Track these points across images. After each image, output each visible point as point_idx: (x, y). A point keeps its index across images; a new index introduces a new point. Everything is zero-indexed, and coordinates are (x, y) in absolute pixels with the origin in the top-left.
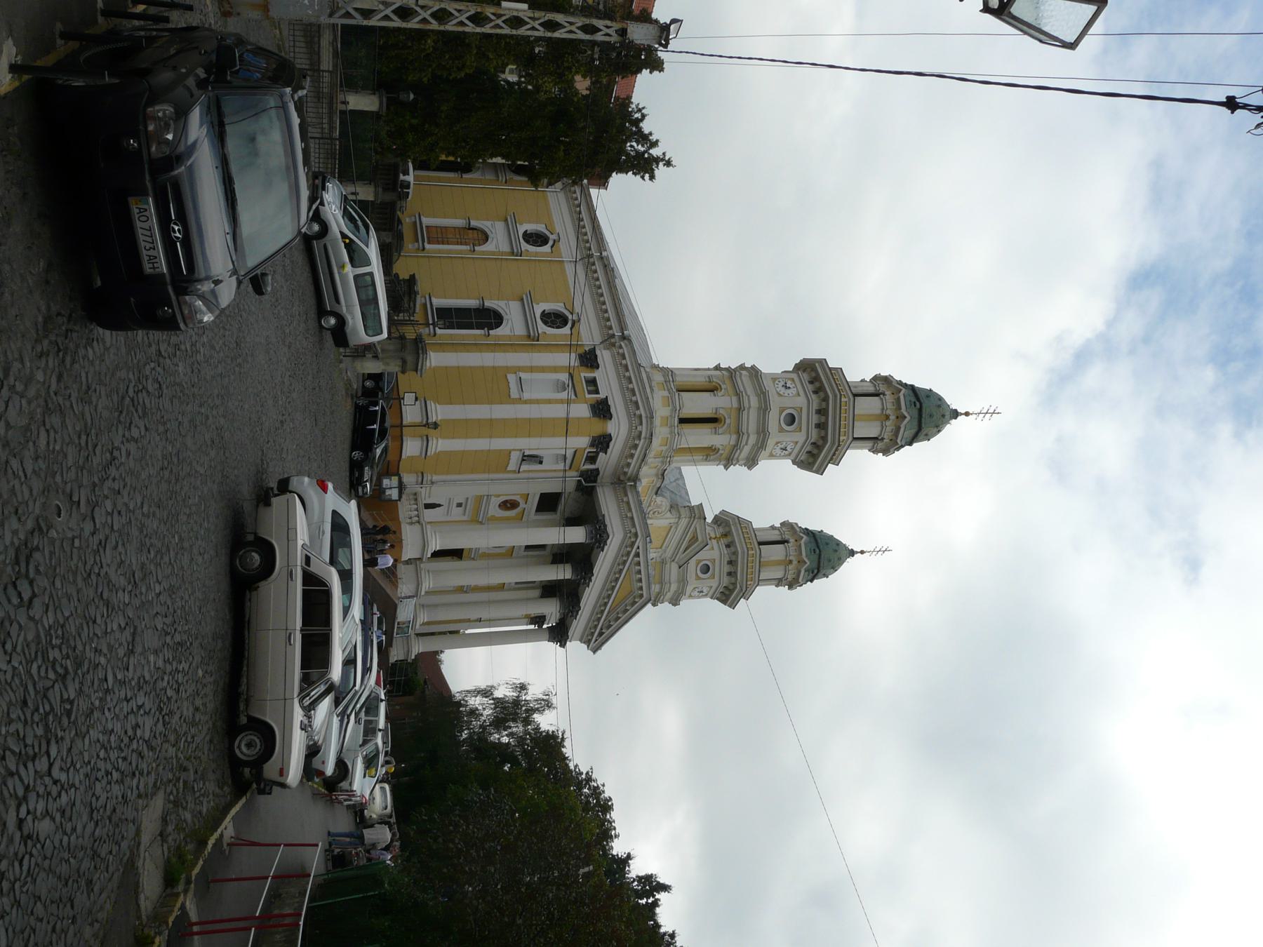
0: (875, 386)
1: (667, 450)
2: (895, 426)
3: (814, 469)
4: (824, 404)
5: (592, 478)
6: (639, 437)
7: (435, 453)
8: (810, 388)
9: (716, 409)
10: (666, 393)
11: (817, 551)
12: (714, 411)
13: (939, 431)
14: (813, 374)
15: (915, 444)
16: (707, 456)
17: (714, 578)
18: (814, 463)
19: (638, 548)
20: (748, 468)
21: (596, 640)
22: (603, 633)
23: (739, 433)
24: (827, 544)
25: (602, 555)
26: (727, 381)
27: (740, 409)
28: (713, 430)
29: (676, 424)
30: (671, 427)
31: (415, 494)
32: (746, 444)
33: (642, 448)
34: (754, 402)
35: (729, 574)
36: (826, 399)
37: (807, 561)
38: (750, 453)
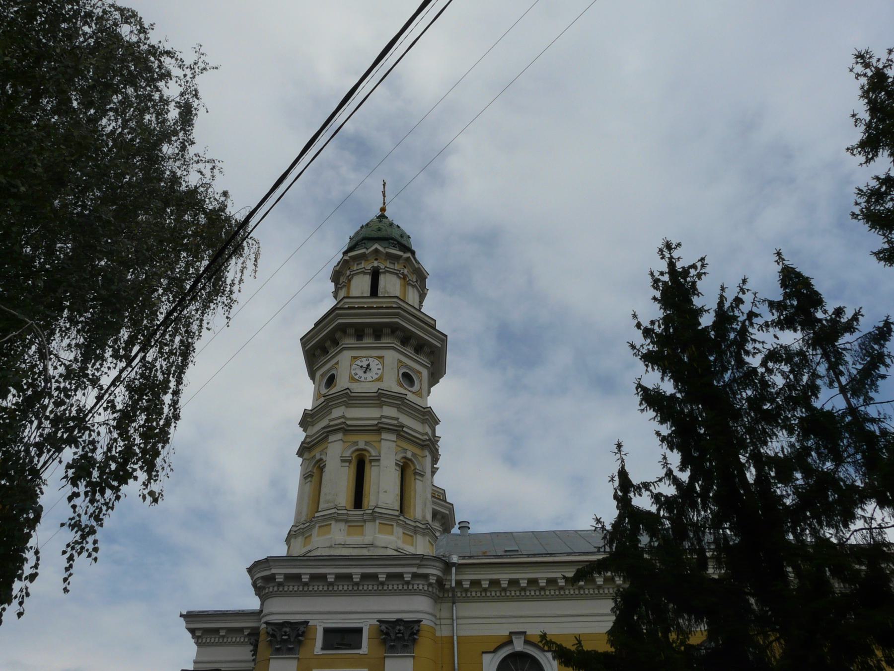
0: (341, 288)
1: (398, 524)
2: (386, 260)
8: (333, 352)
9: (343, 461)
10: (315, 531)
12: (347, 464)
13: (398, 227)
14: (318, 352)
15: (413, 248)
16: (415, 473)
18: (431, 345)
20: (438, 424)
23: (378, 429)
26: (313, 454)
27: (346, 429)
29: (362, 513)
30: (365, 521)
32: (397, 419)
34: (337, 412)
36: (343, 329)
38: (414, 418)
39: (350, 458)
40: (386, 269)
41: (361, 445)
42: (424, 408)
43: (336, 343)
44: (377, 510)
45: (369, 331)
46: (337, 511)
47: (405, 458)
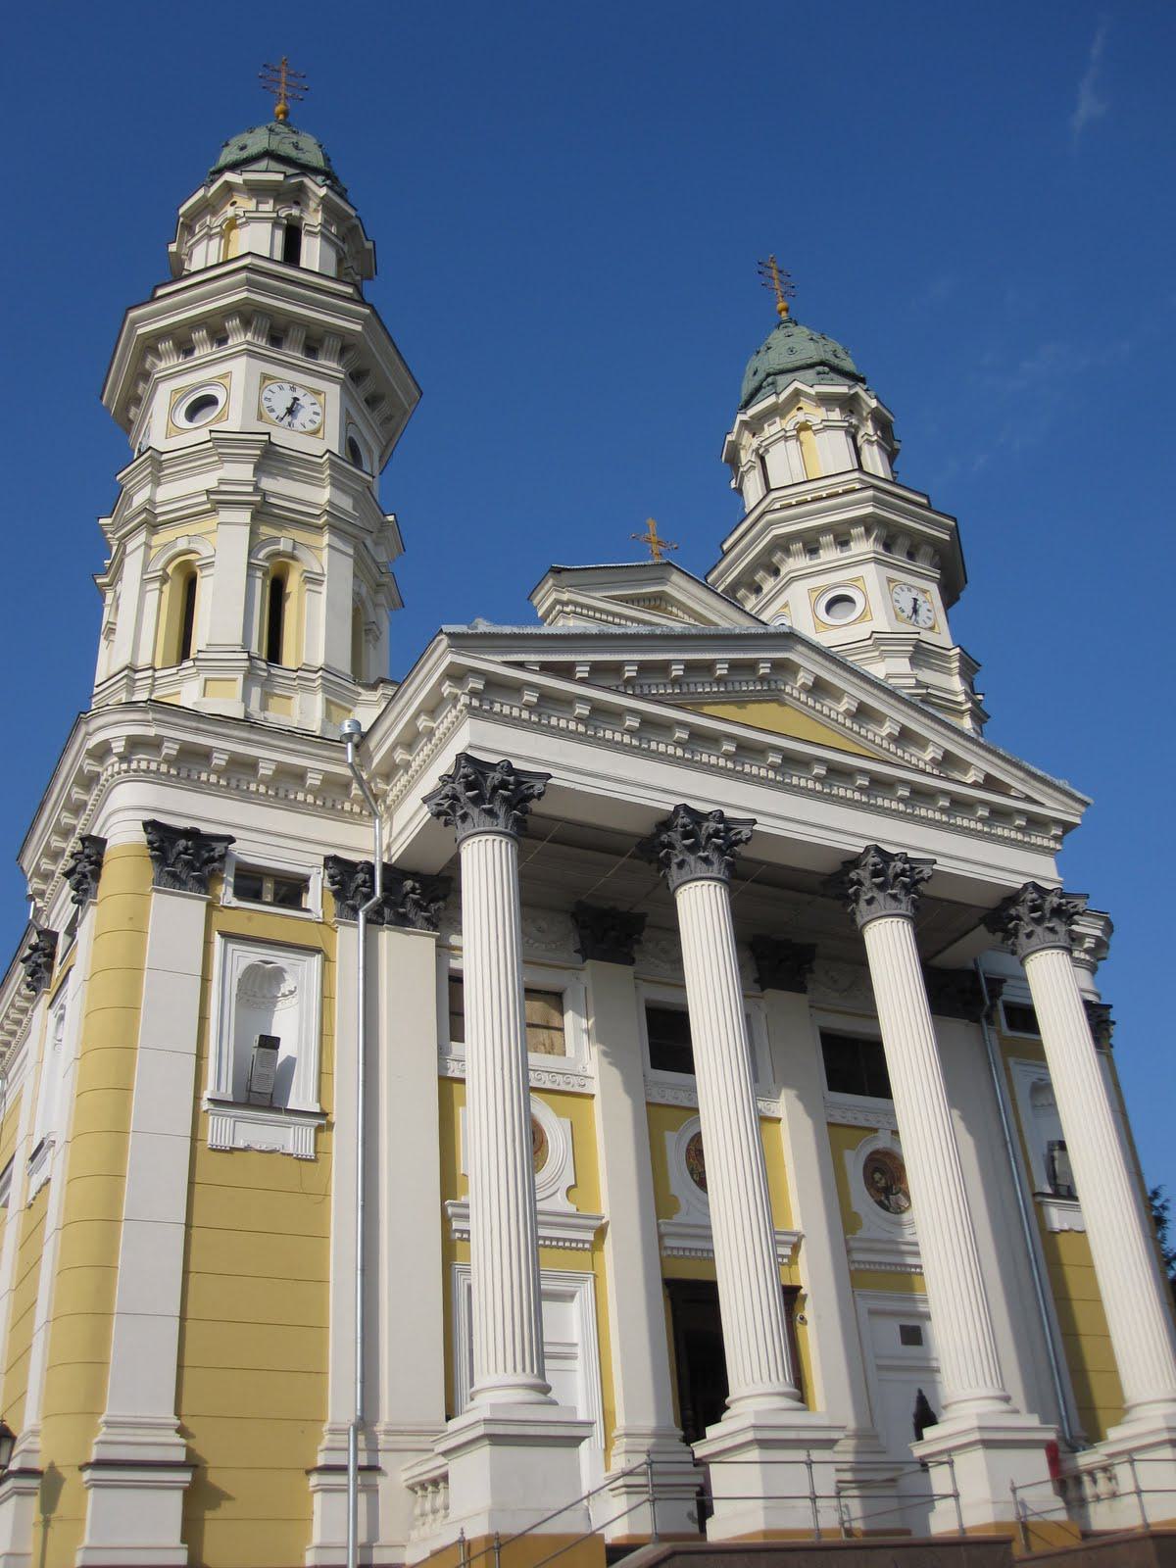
3: (359, 328)
4: (162, 347)
5: (361, 877)
6: (153, 744)
7: (181, 1431)
11: (770, 380)
12: (157, 585)
17: (857, 579)
19: (520, 665)
21: (1029, 799)
22: (988, 777)
24: (755, 374)
25: (560, 779)
28: (206, 572)
30: (181, 682)
31: (412, 1488)
33: (197, 731)
35: (843, 542)
37: (790, 389)
39: (161, 573)
40: (247, 215)
41: (182, 545)
42: (321, 457)
43: (146, 376)
44: (201, 656)
45: (200, 335)
46: (131, 674)
47: (278, 554)
